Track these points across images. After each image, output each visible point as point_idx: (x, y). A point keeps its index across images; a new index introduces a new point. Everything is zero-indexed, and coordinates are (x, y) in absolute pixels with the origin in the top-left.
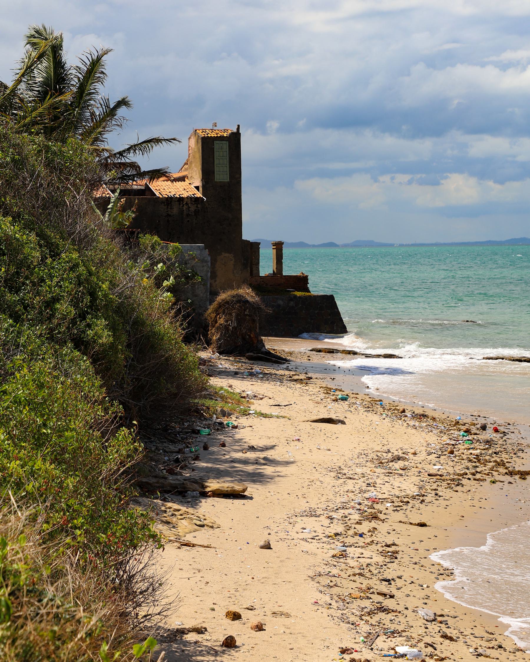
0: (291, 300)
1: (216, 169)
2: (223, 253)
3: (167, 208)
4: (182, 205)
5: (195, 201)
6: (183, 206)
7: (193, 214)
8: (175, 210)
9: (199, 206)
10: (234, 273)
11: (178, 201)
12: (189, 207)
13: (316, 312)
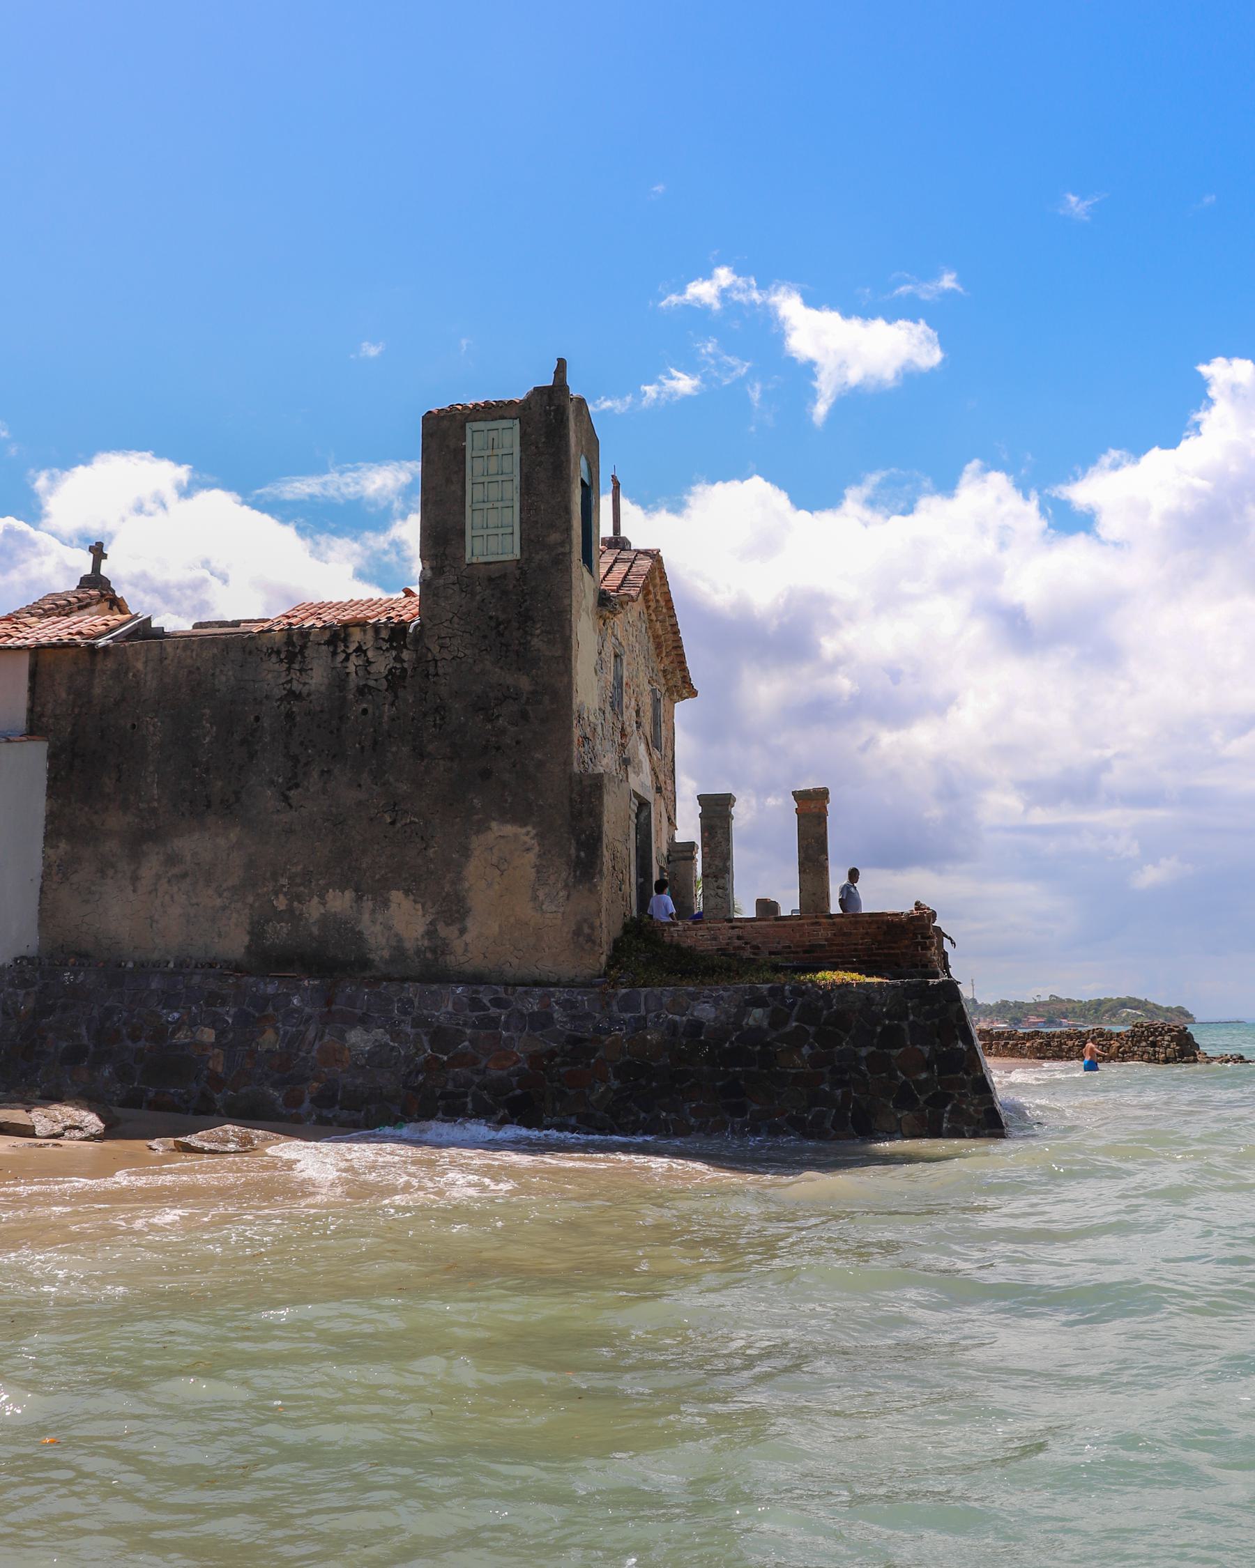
0: (758, 1002)
1: (472, 520)
2: (494, 825)
3: (289, 669)
4: (343, 656)
5: (390, 640)
6: (347, 659)
7: (384, 684)
8: (317, 677)
9: (406, 655)
10: (535, 898)
11: (328, 643)
12: (369, 662)
13: (863, 1052)
